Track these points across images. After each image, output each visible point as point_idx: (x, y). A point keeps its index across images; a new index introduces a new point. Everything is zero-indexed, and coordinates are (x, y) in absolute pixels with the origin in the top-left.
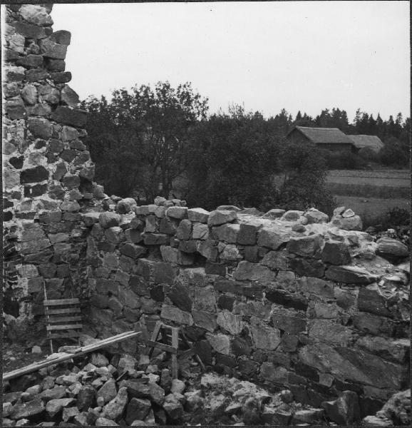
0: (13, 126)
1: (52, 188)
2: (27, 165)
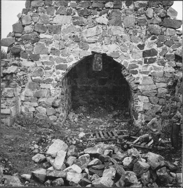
0: (140, 29)
1: (159, 60)
2: (146, 48)
